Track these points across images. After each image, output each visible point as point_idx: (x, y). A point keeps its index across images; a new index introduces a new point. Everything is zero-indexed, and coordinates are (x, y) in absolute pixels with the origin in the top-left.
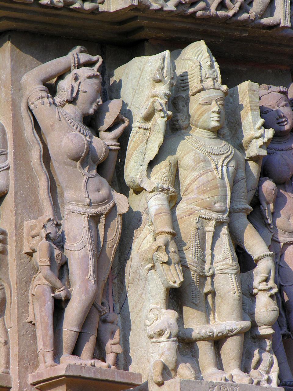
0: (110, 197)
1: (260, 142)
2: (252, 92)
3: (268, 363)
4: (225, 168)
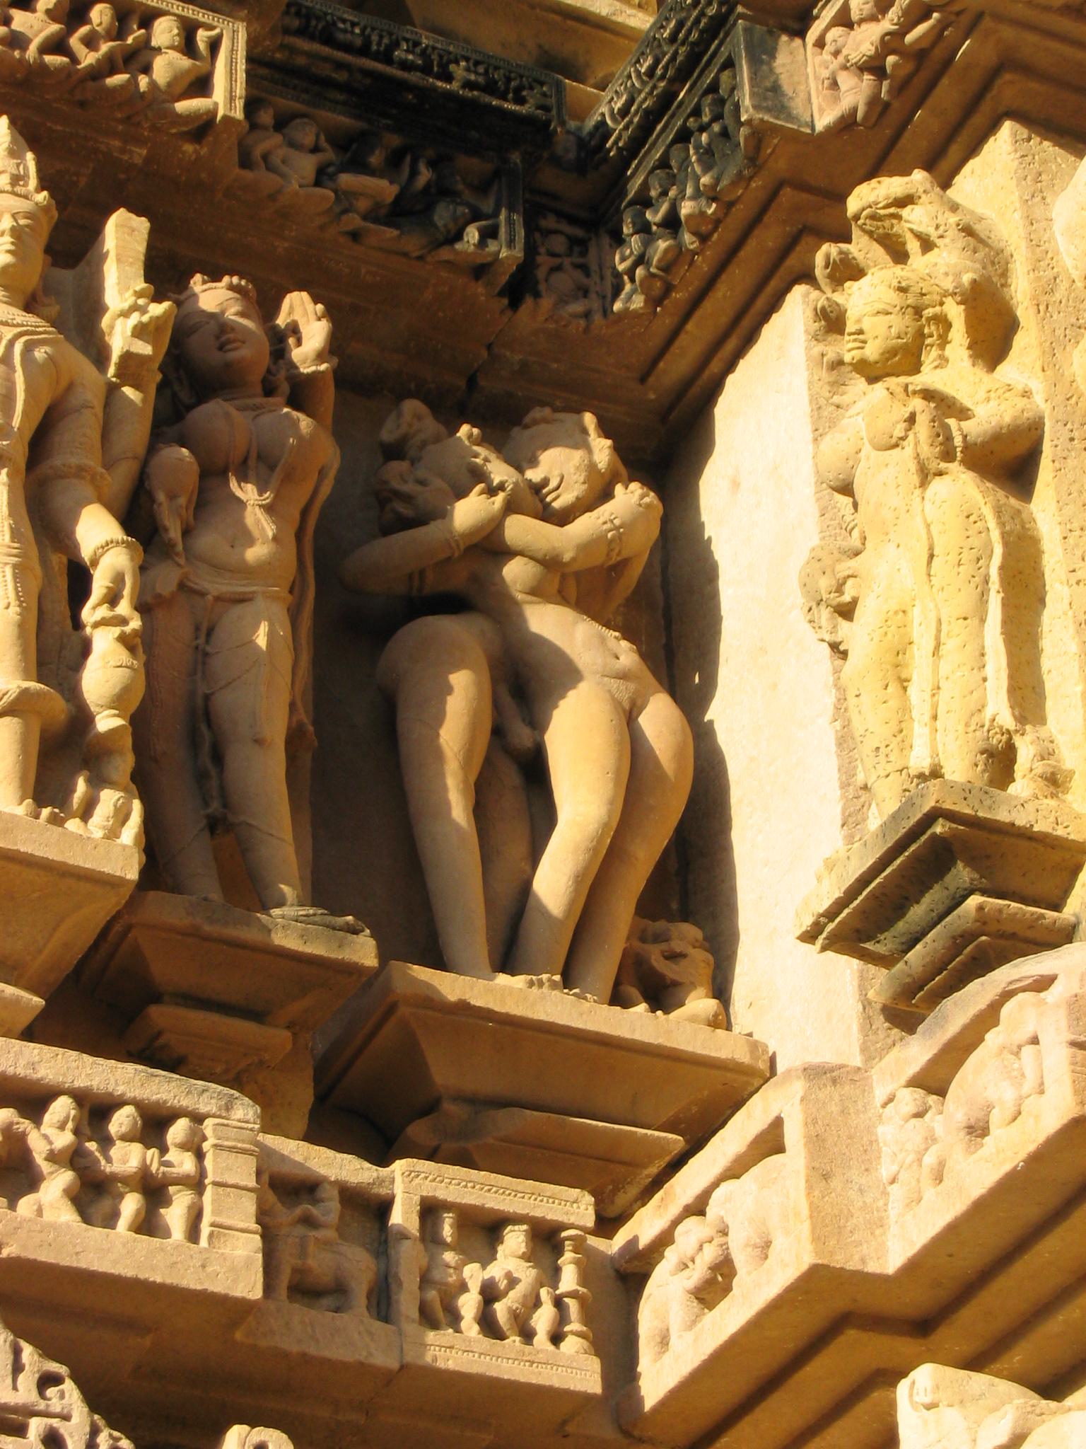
1: (135, 318)
2: (126, 230)
3: (112, 808)
4: (18, 347)
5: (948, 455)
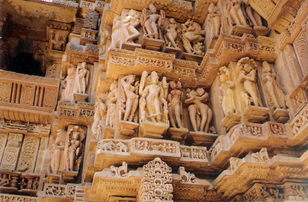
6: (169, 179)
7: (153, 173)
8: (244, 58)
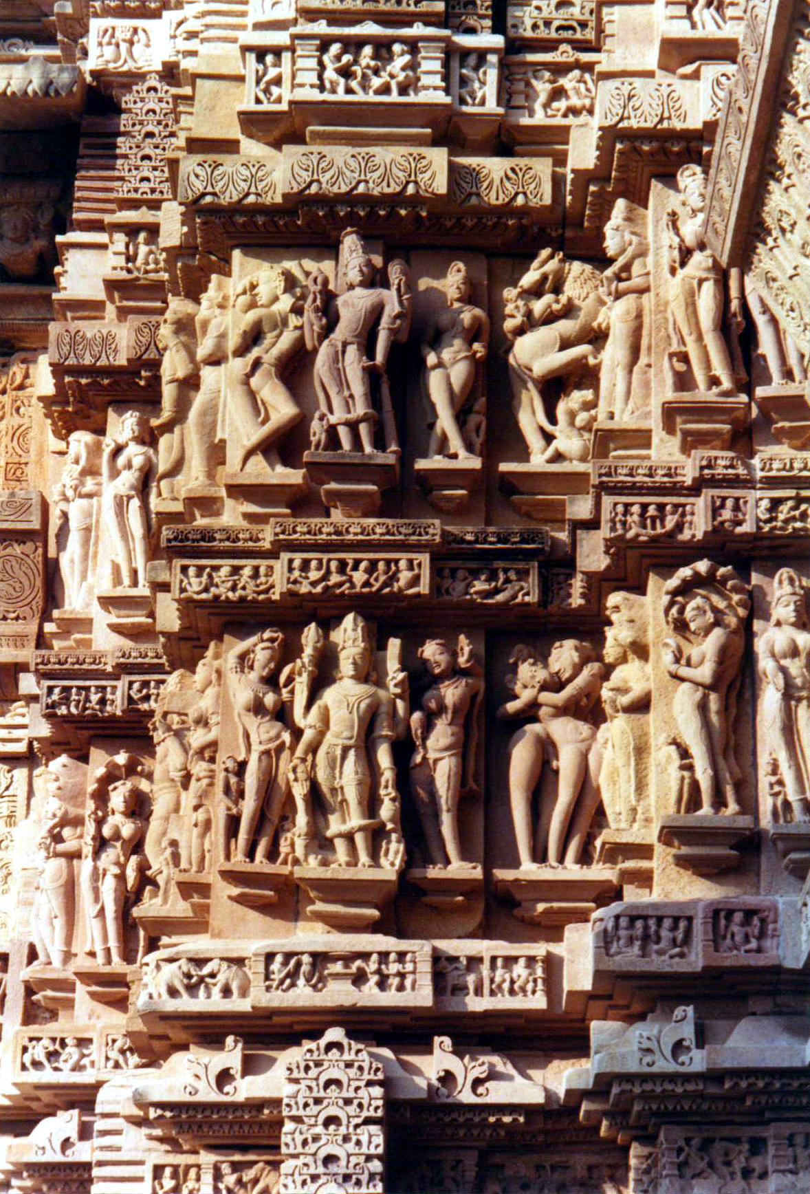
0: (278, 736)
5: (617, 711)
6: (372, 1109)
7: (315, 1089)
8: (685, 572)
